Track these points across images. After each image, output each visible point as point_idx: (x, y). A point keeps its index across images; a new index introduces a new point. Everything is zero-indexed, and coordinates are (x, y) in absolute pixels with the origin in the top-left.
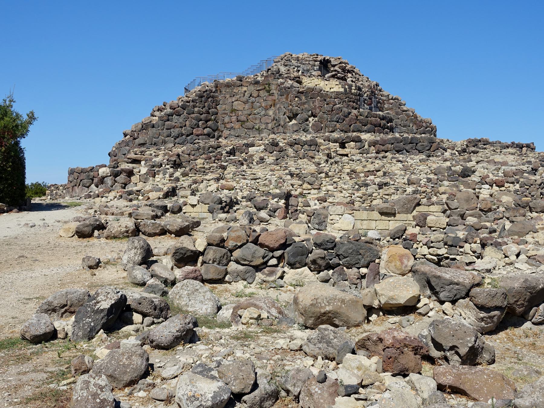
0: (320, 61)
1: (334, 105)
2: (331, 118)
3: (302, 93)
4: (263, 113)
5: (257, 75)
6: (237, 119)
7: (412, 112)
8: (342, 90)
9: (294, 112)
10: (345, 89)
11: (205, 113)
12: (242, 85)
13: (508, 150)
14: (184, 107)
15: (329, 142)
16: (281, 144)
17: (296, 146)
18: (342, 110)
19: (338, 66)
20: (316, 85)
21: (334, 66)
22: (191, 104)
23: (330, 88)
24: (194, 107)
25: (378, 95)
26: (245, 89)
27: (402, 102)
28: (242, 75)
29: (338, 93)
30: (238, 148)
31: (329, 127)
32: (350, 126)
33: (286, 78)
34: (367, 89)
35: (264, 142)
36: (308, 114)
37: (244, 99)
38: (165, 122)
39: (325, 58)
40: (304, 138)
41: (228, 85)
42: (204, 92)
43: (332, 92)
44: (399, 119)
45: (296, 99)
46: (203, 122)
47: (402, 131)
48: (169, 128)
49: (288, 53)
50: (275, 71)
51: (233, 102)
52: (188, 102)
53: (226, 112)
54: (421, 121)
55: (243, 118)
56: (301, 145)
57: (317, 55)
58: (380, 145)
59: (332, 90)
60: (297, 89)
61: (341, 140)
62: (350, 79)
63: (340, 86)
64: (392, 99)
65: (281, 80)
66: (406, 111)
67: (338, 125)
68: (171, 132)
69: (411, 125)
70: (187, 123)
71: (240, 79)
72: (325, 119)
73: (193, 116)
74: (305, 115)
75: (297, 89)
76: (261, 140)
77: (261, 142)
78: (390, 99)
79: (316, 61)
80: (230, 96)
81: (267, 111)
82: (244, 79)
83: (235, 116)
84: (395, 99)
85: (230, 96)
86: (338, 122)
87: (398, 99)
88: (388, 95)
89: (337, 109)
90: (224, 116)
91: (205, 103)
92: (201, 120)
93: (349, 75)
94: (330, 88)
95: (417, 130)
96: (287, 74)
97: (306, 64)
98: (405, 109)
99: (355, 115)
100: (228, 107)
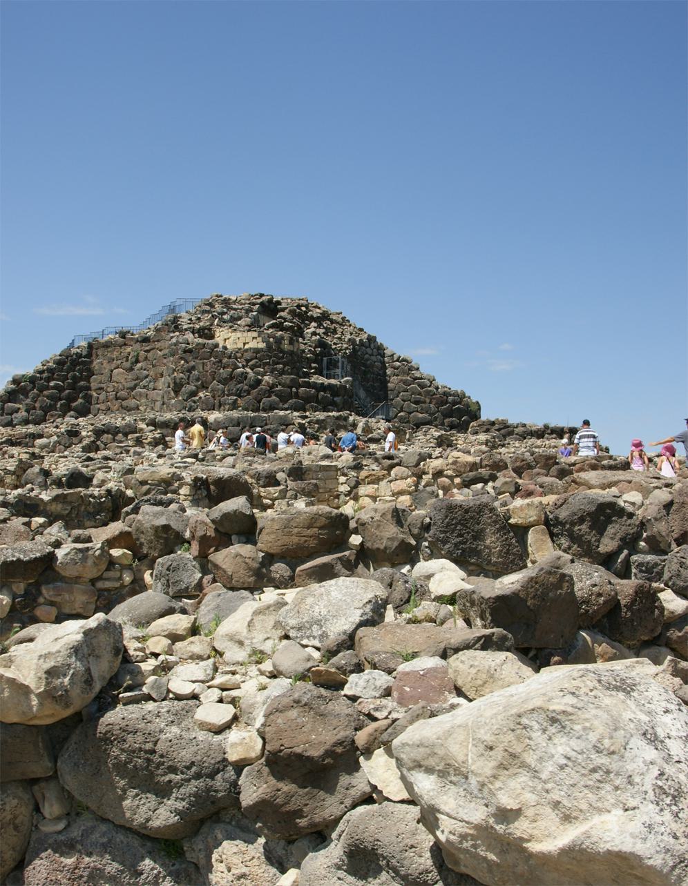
0: (262, 304)
1: (233, 370)
2: (229, 390)
3: (190, 351)
4: (151, 385)
5: (149, 328)
6: (116, 395)
7: (429, 380)
8: (262, 345)
9: (178, 381)
10: (268, 343)
11: (67, 389)
12: (125, 345)
13: (478, 437)
14: (32, 380)
15: (153, 428)
16: (84, 434)
17: (106, 435)
18: (246, 377)
19: (287, 311)
20: (225, 340)
21: (283, 310)
22: (45, 375)
23: (244, 344)
24: (49, 380)
25: (370, 355)
26: (129, 349)
27: (413, 364)
28: (125, 329)
29: (257, 351)
30: (18, 440)
31: (225, 404)
32: (259, 402)
33: (186, 330)
34: (345, 346)
35: (58, 430)
36: (196, 384)
37: (128, 365)
38: (4, 404)
39: (270, 301)
40: (119, 423)
41: (107, 345)
42: (67, 357)
43: (246, 351)
44: (407, 391)
45: (183, 362)
46: (62, 402)
47: (411, 411)
48: (10, 412)
49: (215, 294)
50: (170, 321)
51: (112, 371)
52: (41, 372)
53: (102, 385)
54: (446, 394)
55: (123, 393)
56: (112, 434)
57: (262, 295)
58: (213, 430)
59: (246, 347)
60: (183, 345)
61: (173, 425)
62: (313, 330)
63: (260, 339)
64: (398, 361)
65: (177, 333)
66: (421, 379)
67: (239, 401)
68: (12, 419)
69: (428, 400)
70: (37, 405)
71: (123, 335)
72: (220, 392)
73: (45, 393)
74: (192, 387)
75: (183, 345)
76: (57, 427)
77: (55, 429)
78: (395, 361)
79: (254, 304)
80: (109, 362)
81: (156, 384)
82: (129, 336)
83: (113, 391)
84: (404, 360)
85: (109, 362)
86: (240, 396)
87: (407, 361)
88: (392, 355)
89: (239, 376)
90: (99, 392)
91: (68, 373)
92: (60, 399)
93: (313, 324)
94: (244, 344)
95: (438, 408)
96: (190, 324)
97: (238, 309)
98: (417, 374)
99: (268, 383)
100: (104, 378)
